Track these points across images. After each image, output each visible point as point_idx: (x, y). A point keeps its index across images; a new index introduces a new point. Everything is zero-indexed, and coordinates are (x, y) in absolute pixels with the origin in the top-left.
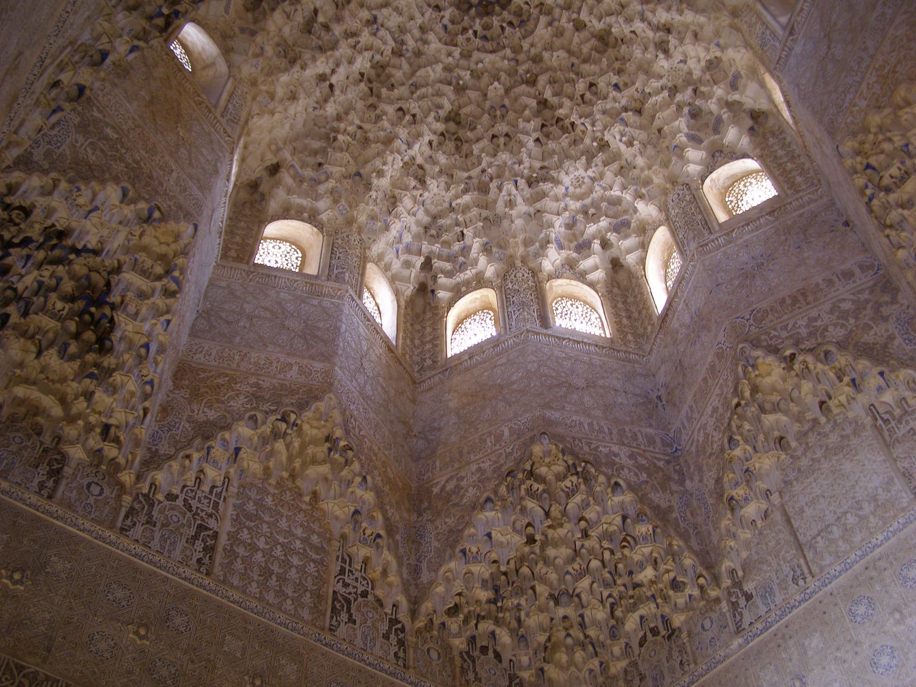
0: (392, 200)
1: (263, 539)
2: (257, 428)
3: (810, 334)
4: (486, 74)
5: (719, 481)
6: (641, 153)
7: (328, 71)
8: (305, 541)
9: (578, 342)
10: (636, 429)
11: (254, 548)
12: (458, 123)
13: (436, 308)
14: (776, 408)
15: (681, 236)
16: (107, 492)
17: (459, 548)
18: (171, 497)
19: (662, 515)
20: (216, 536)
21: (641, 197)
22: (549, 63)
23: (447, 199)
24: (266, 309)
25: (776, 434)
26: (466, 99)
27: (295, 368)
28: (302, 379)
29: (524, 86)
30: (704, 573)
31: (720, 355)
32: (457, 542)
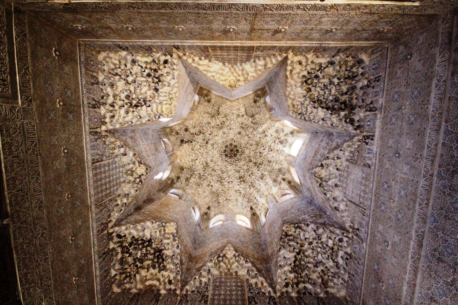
1: (223, 291)
3: (322, 157)
5: (330, 206)
8: (236, 286)
10: (308, 210)
11: (220, 295)
14: (330, 179)
16: (173, 299)
18: (193, 292)
19: (324, 225)
20: (208, 296)
25: (334, 185)
30: (343, 231)
31: (310, 179)
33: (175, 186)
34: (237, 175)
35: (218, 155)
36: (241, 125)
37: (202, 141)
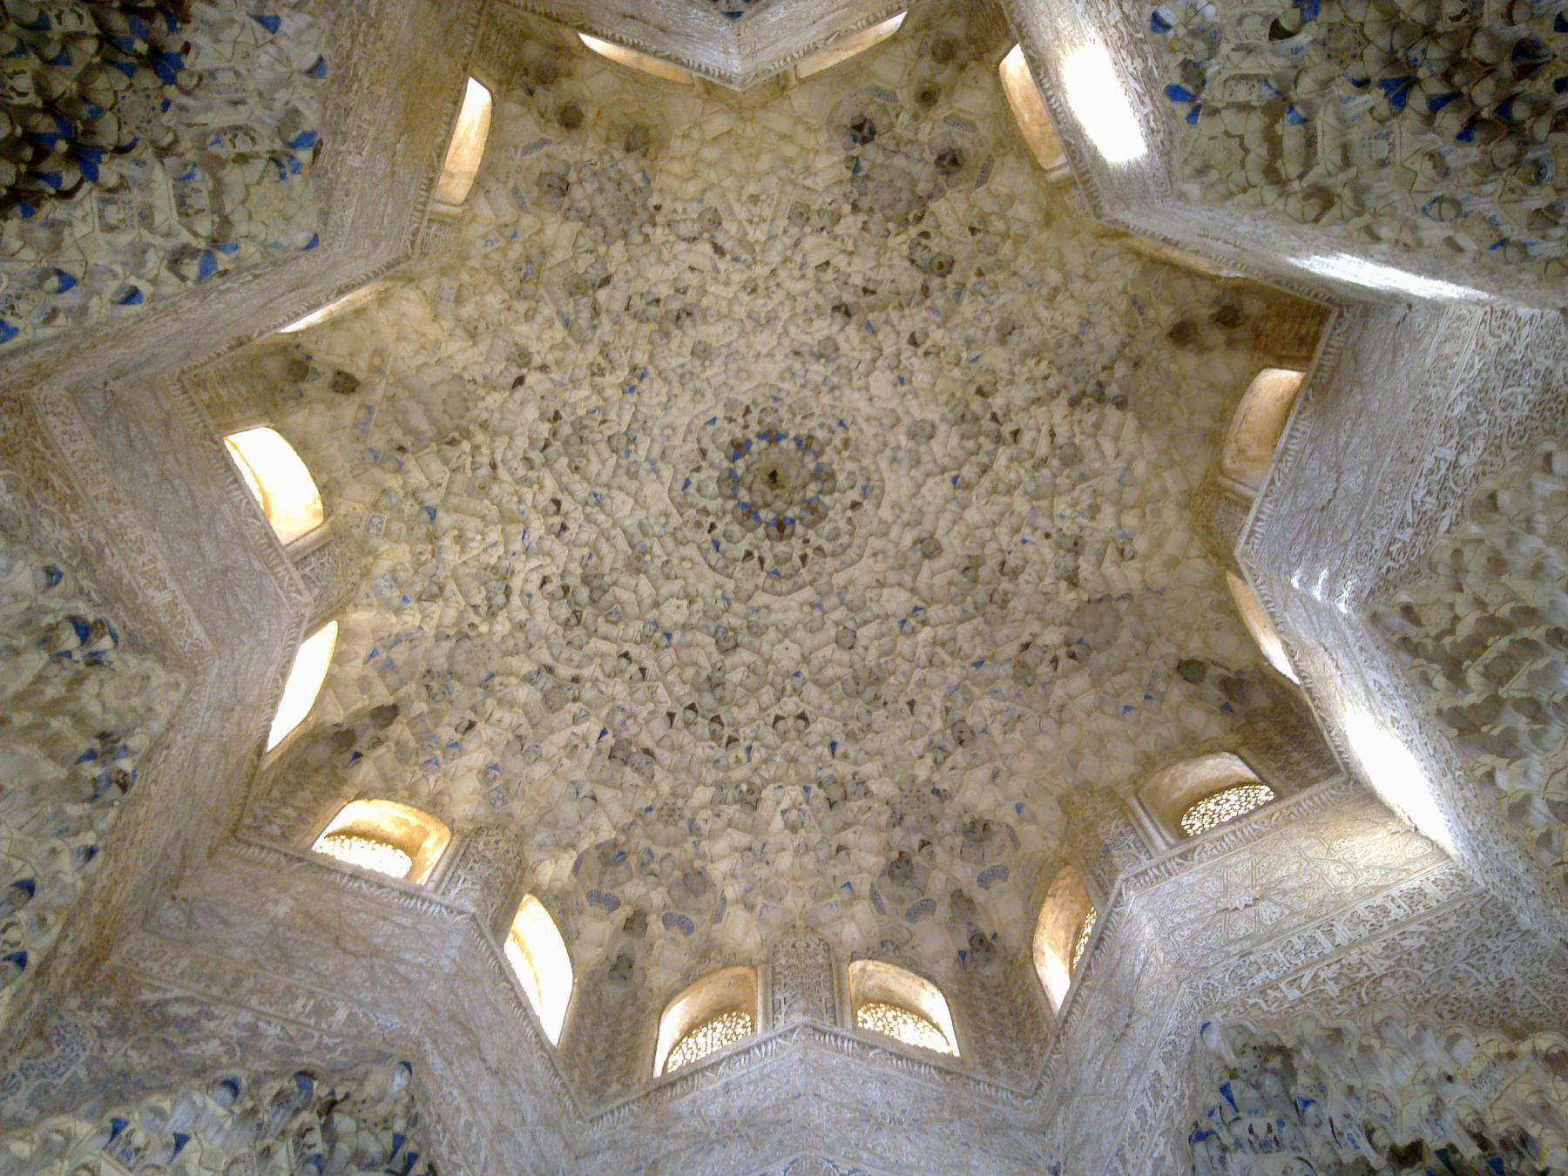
0: (435, 590)
2: (43, 593)
4: (681, 582)
6: (797, 852)
7: (537, 361)
9: (519, 1005)
12: (593, 601)
13: (344, 781)
15: (779, 996)
17: (119, 1112)
21: (750, 908)
22: (766, 647)
23: (493, 667)
24: (192, 495)
26: (632, 582)
27: (166, 597)
28: (165, 620)
29: (713, 640)
32: (123, 1099)
33: (512, 108)
34: (612, 556)
35: (744, 392)
36: (992, 563)
37: (857, 280)
